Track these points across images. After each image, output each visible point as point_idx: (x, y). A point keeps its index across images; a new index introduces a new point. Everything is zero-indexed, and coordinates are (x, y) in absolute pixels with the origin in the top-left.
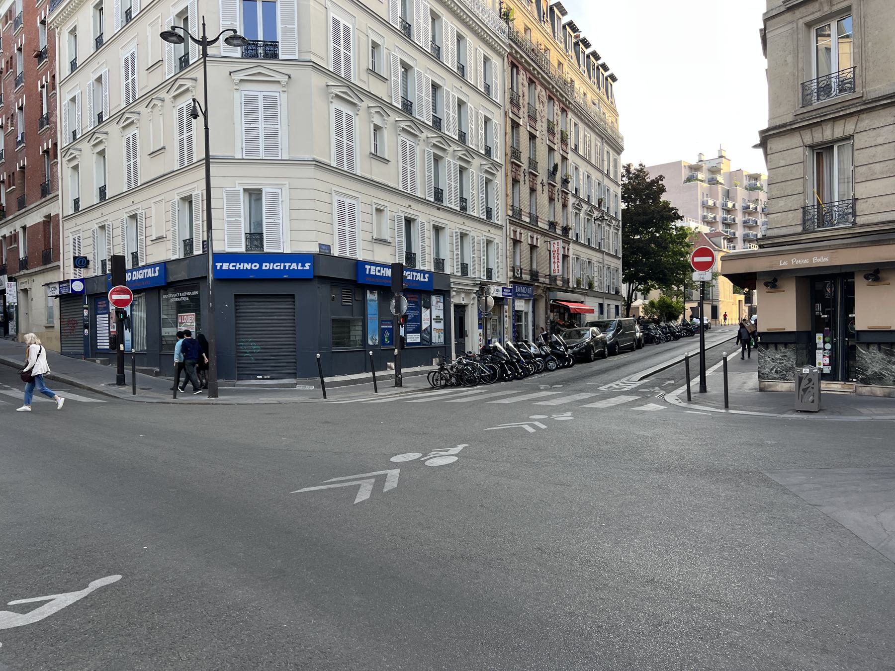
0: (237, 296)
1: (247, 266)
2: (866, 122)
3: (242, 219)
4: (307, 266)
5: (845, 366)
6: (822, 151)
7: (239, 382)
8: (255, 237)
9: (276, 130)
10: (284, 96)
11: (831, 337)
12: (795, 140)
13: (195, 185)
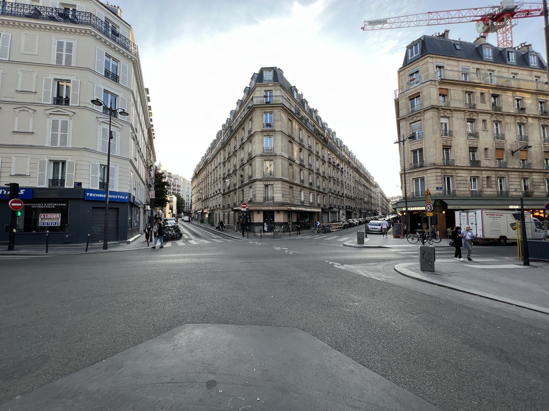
0: (93, 208)
1: (101, 196)
2: (276, 183)
3: (66, 174)
4: (127, 197)
5: (270, 229)
6: (266, 186)
7: (93, 244)
8: (104, 185)
9: (52, 131)
10: (71, 121)
11: (267, 224)
12: (262, 183)
13: (70, 157)
